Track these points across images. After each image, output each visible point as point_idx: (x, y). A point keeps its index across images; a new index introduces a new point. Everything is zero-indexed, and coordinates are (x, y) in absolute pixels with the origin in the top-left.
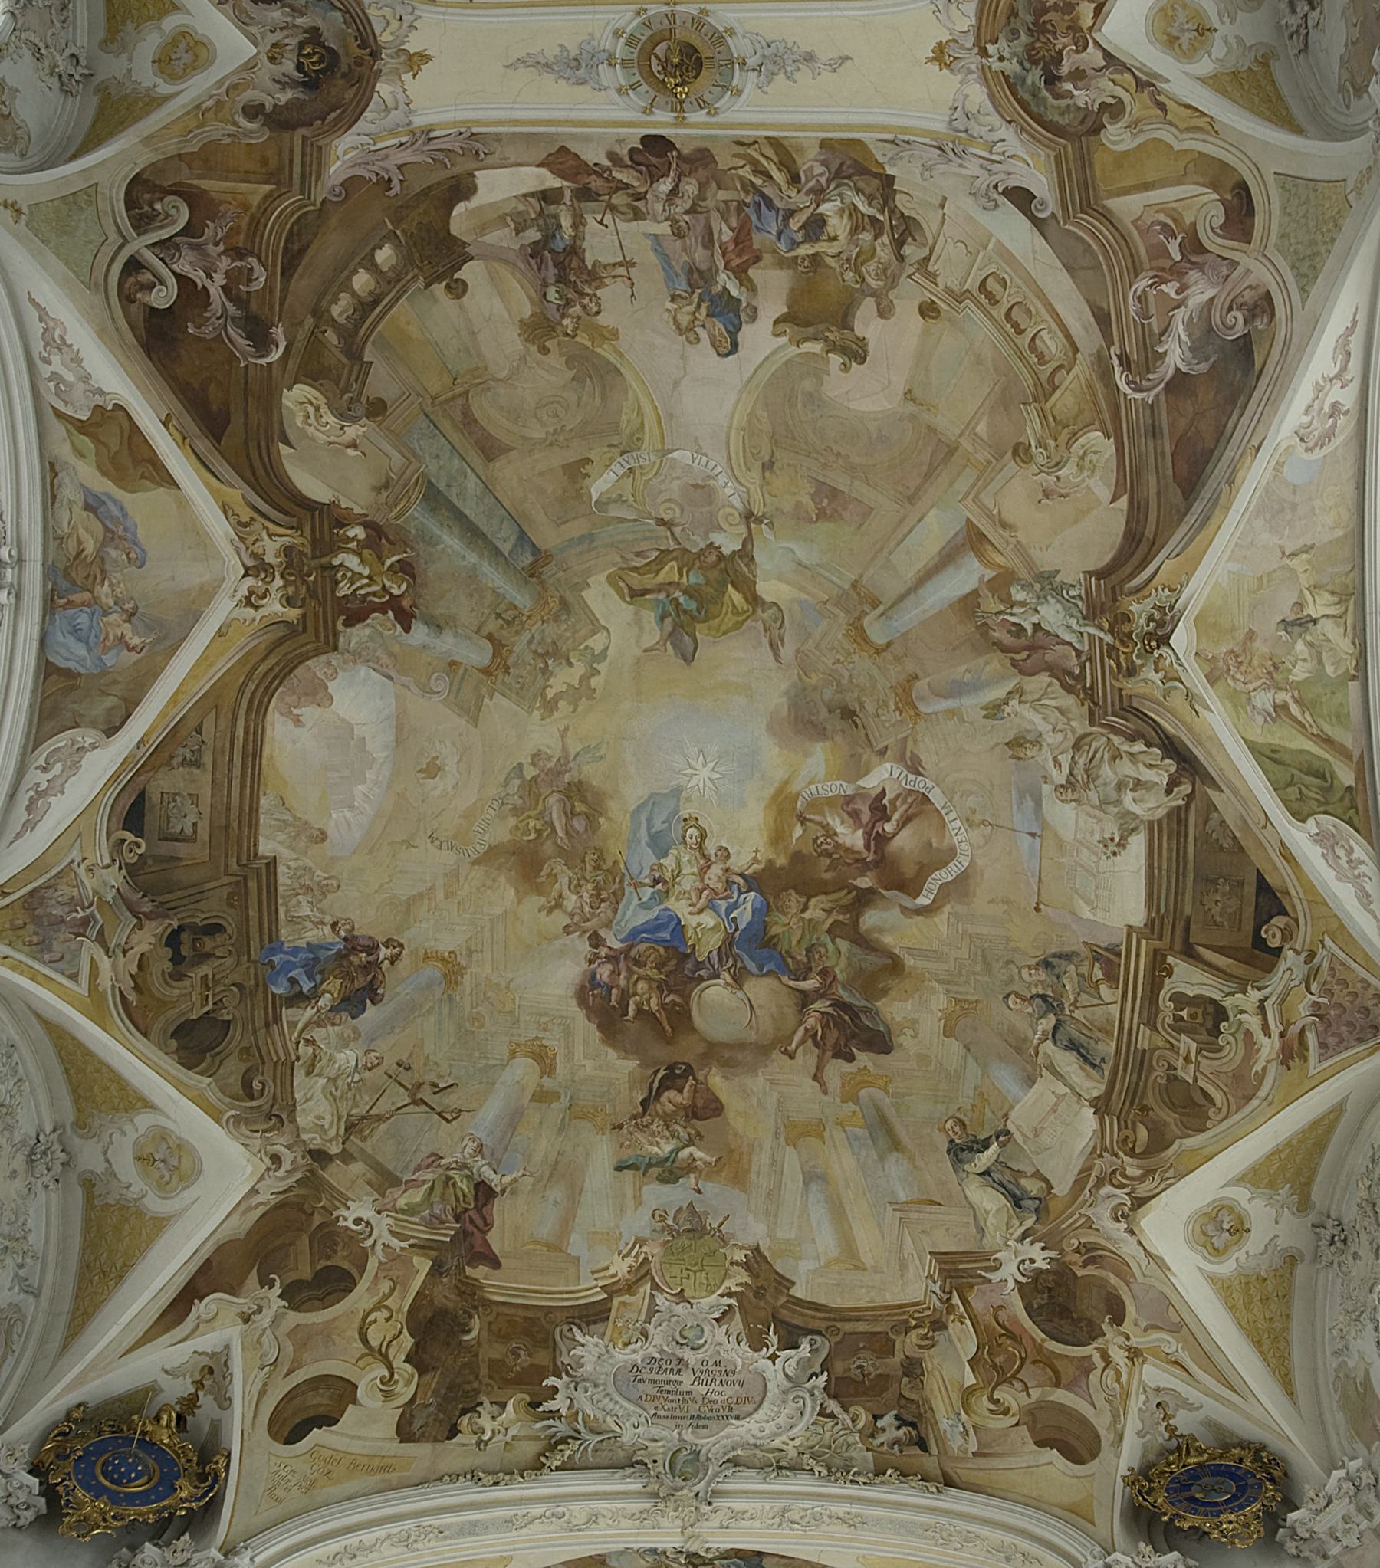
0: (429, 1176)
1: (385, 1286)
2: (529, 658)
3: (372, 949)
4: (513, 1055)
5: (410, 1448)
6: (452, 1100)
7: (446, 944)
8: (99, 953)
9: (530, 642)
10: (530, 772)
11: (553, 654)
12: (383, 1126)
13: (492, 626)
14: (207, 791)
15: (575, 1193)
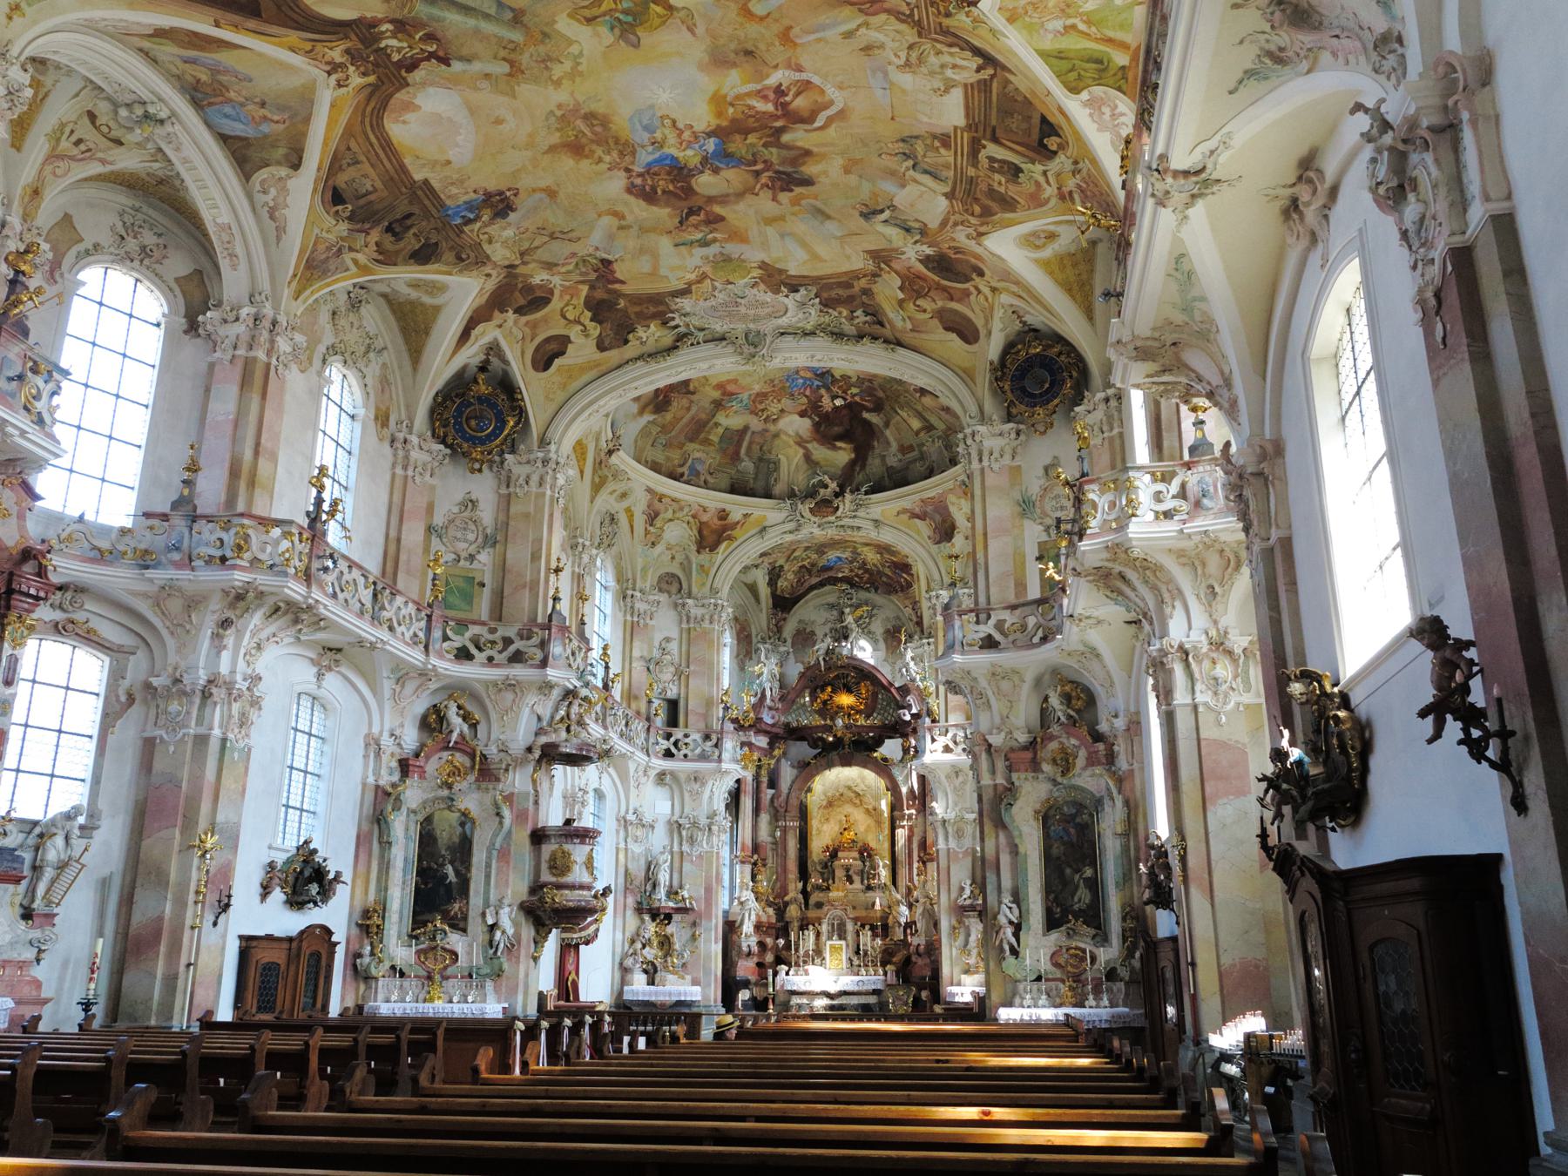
0: (574, 261)
1: (568, 297)
2: (534, 64)
3: (501, 193)
4: (600, 216)
5: (606, 354)
6: (573, 235)
7: (543, 184)
8: (353, 255)
9: (531, 56)
10: (559, 113)
11: (546, 61)
12: (540, 251)
13: (503, 53)
14: (370, 171)
15: (655, 256)
